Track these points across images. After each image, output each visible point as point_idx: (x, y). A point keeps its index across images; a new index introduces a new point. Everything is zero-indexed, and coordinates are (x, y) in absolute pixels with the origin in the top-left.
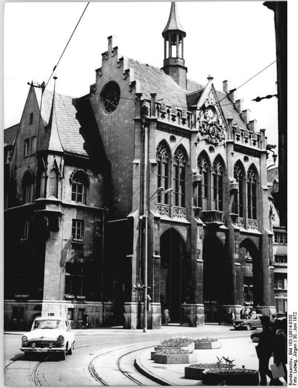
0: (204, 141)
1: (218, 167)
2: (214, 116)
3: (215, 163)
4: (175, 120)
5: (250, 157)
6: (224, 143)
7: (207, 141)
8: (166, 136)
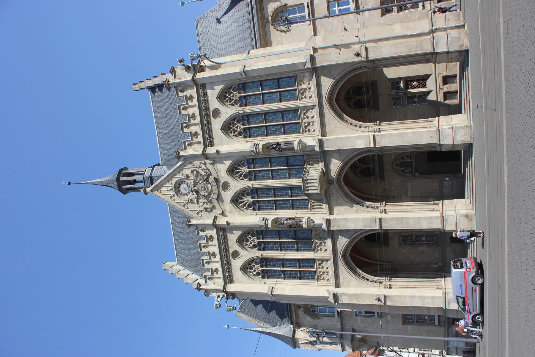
5: (212, 108)
6: (210, 164)
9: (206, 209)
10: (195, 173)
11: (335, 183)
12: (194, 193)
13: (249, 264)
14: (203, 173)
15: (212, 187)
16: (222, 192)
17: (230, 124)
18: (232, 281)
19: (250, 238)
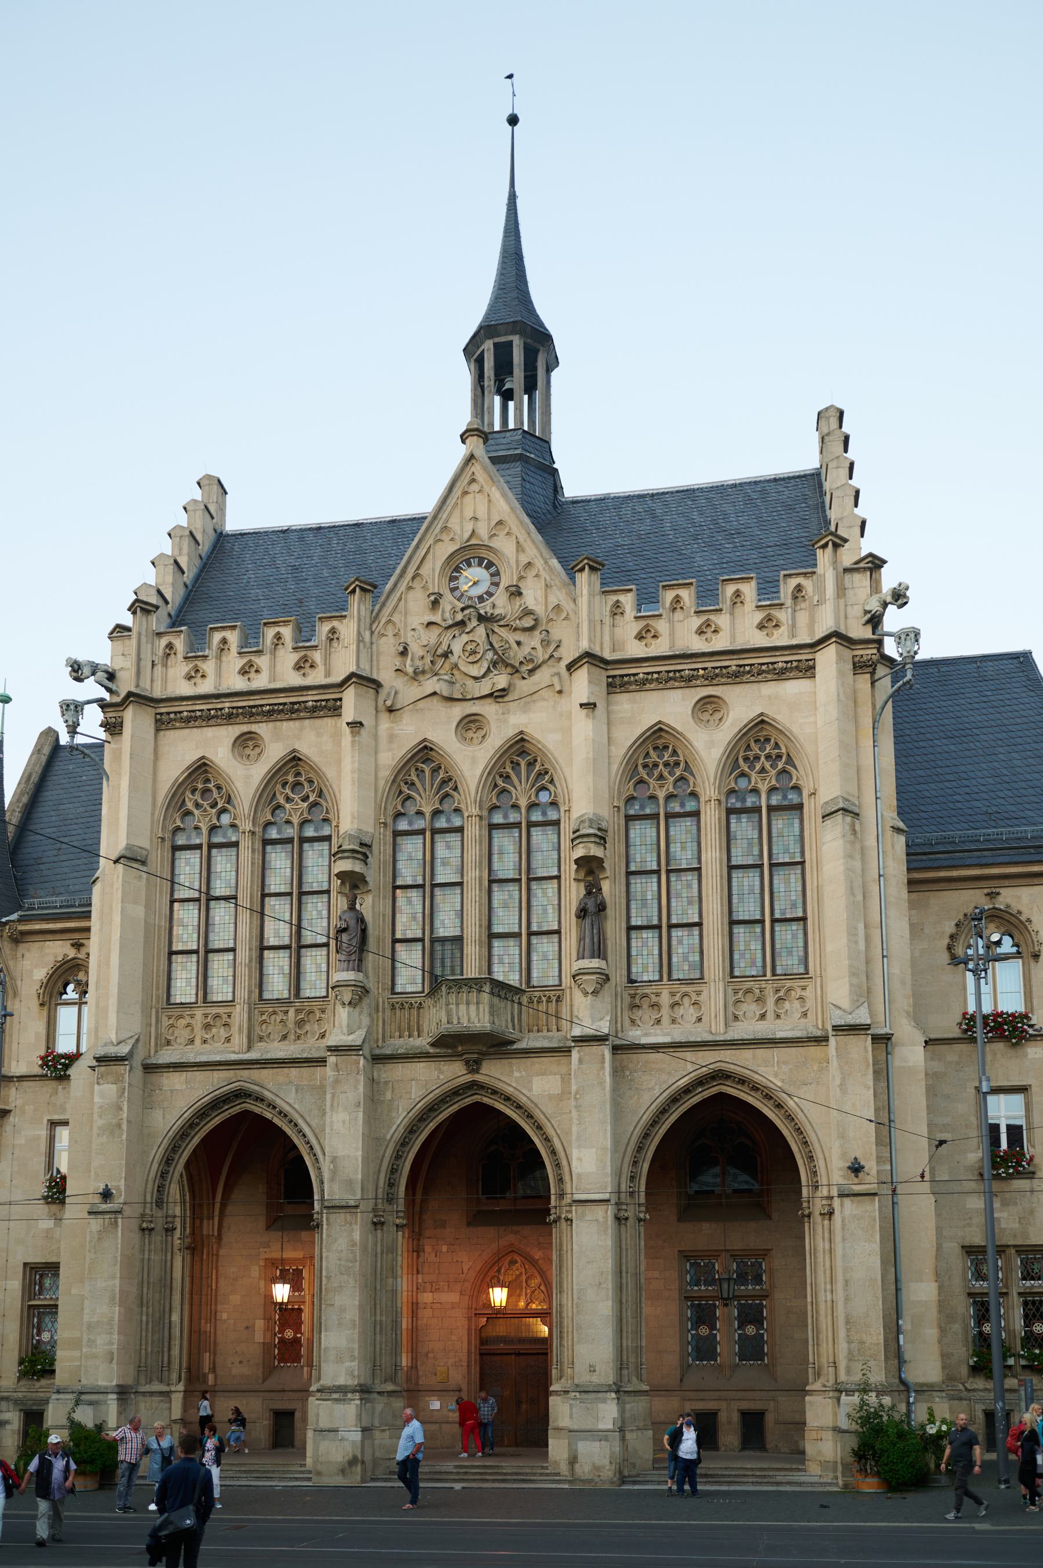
2: (497, 584)
9: (404, 653)
10: (528, 622)
11: (469, 1078)
12: (459, 617)
13: (219, 788)
14: (526, 650)
15: (475, 678)
16: (458, 711)
17: (675, 753)
18: (162, 724)
19: (305, 799)
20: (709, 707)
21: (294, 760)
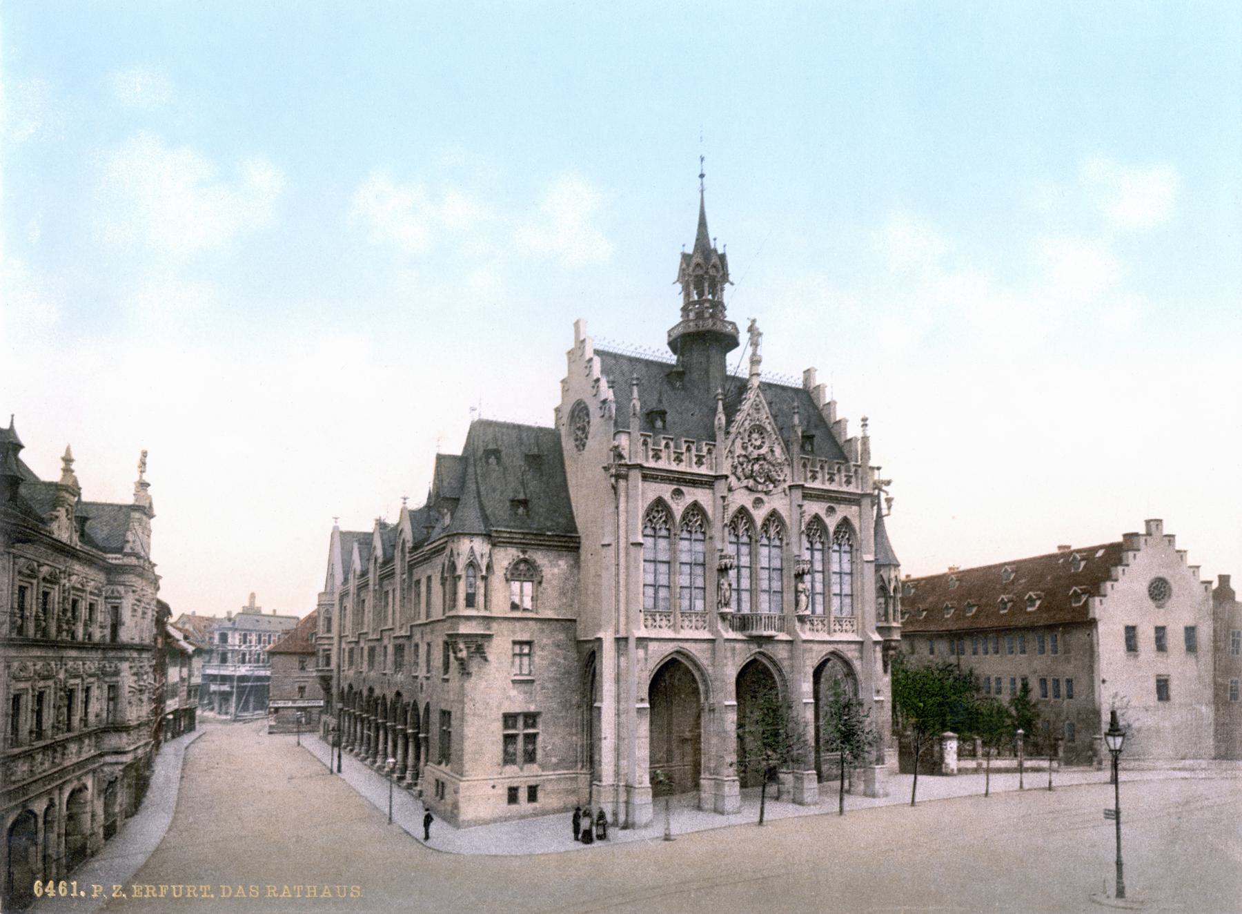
0: (743, 491)
1: (772, 532)
3: (765, 525)
4: (681, 461)
7: (747, 488)
8: (665, 491)
20: (831, 510)
21: (695, 504)
